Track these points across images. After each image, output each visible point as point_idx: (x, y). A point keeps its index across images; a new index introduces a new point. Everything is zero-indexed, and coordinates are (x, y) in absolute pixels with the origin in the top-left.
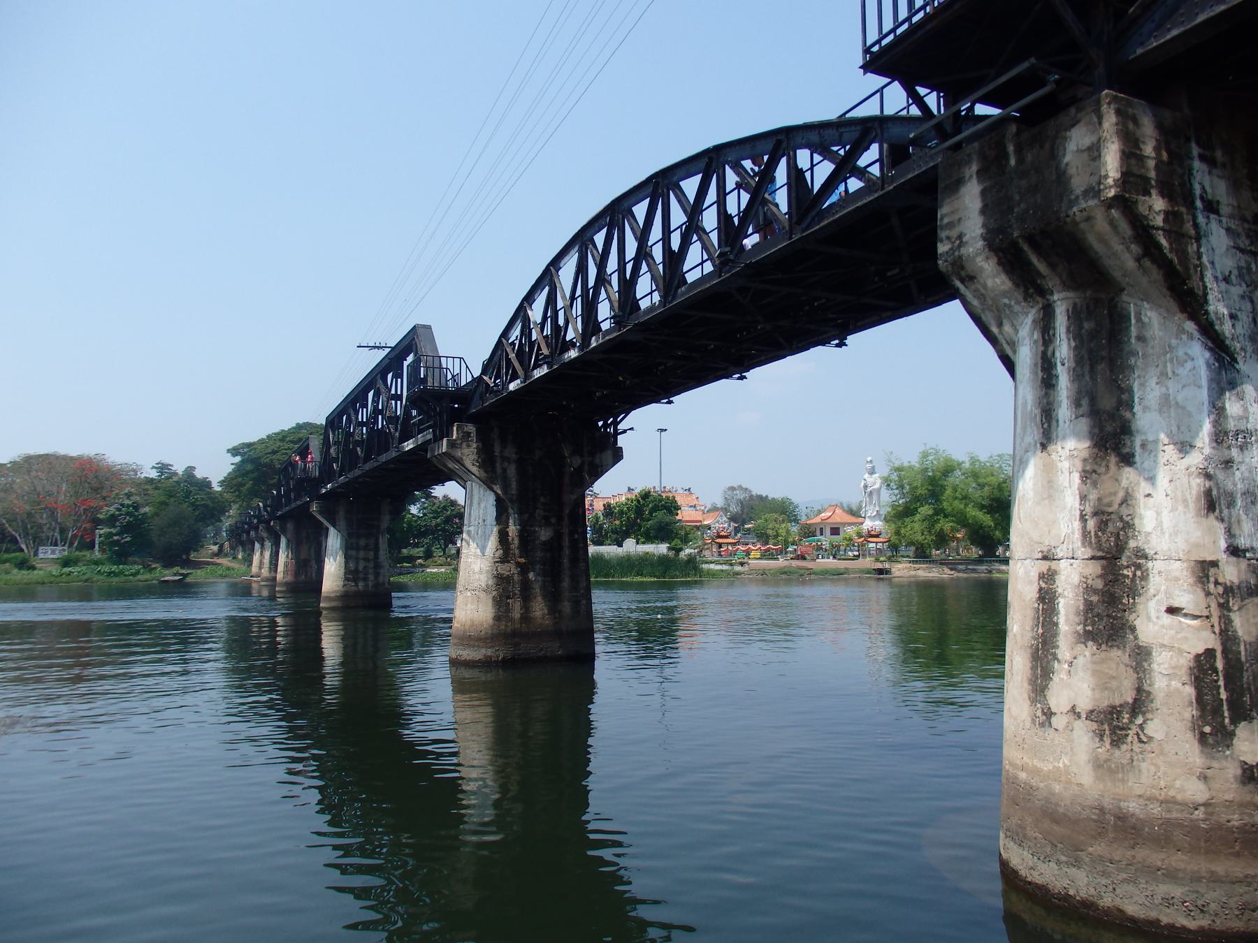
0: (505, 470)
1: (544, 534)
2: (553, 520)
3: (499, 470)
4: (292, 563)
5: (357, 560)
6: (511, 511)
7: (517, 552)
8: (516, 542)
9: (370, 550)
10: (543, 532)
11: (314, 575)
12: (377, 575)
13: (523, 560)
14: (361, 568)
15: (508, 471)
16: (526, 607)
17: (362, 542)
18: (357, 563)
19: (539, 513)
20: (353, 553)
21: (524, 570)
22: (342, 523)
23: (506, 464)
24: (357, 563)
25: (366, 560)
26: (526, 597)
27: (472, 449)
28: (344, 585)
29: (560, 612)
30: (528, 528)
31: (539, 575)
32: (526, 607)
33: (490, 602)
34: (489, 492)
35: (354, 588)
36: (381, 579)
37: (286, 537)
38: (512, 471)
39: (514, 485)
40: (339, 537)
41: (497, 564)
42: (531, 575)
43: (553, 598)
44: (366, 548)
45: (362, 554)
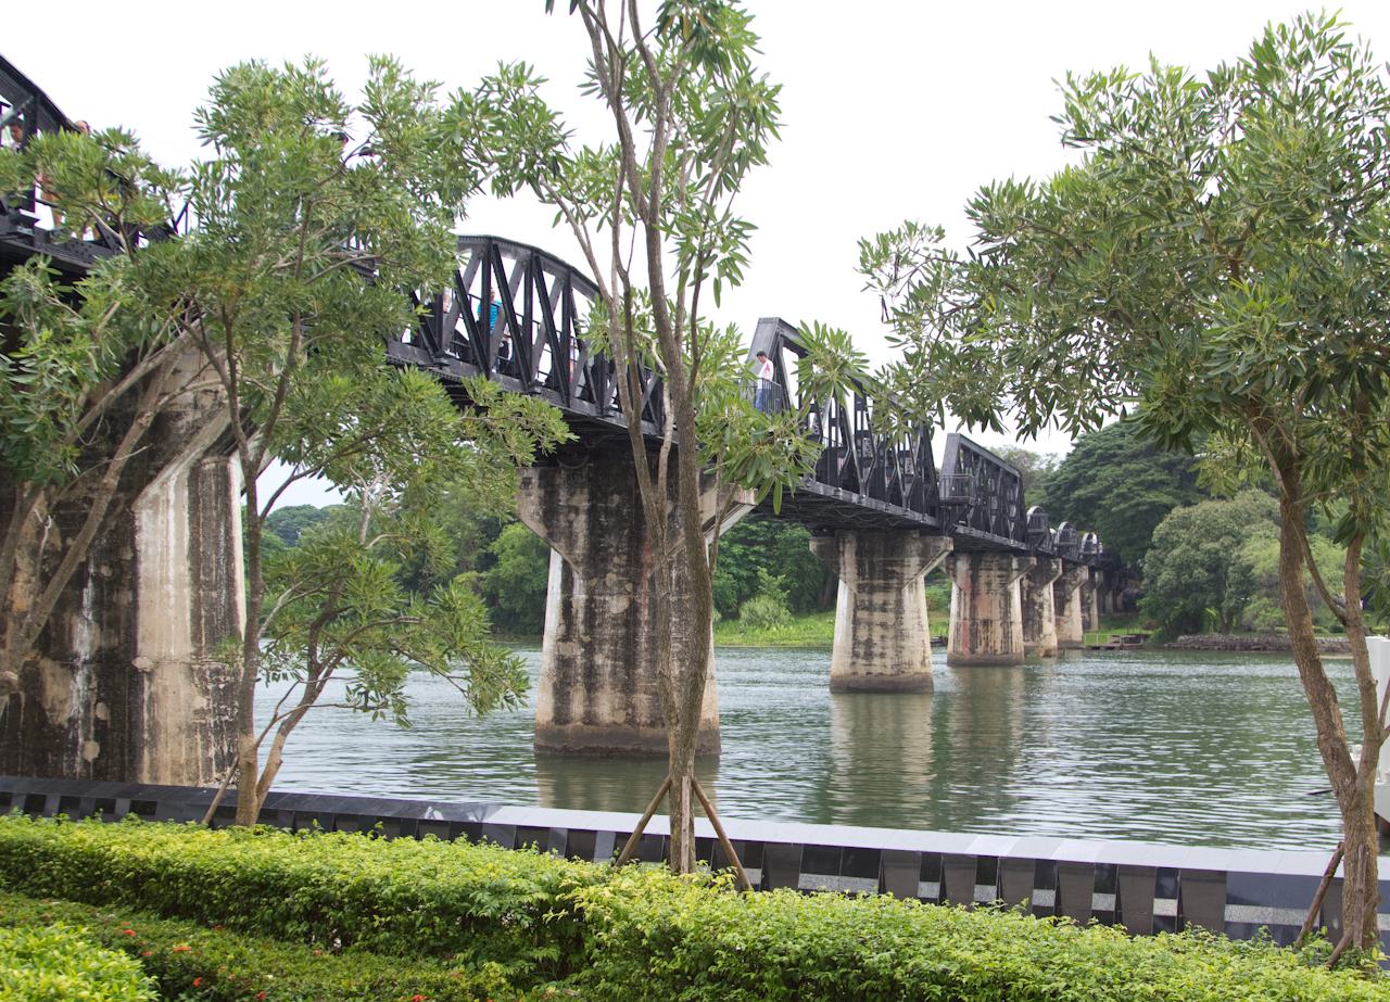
0: (571, 523)
1: (617, 605)
2: (629, 587)
3: (563, 524)
4: (965, 625)
5: (870, 624)
6: (576, 576)
7: (581, 628)
8: (581, 615)
10: (614, 602)
11: (998, 645)
12: (899, 650)
13: (587, 639)
14: (876, 639)
16: (590, 701)
17: (878, 598)
18: (870, 630)
19: (611, 578)
20: (862, 614)
21: (590, 650)
23: (572, 516)
24: (870, 630)
25: (883, 625)
26: (591, 688)
28: (854, 663)
29: (634, 707)
30: (597, 598)
31: (608, 657)
32: (590, 701)
33: (551, 689)
35: (862, 671)
36: (906, 656)
38: (581, 524)
39: (581, 542)
42: (599, 659)
43: (628, 688)
44: (884, 609)
45: (878, 617)
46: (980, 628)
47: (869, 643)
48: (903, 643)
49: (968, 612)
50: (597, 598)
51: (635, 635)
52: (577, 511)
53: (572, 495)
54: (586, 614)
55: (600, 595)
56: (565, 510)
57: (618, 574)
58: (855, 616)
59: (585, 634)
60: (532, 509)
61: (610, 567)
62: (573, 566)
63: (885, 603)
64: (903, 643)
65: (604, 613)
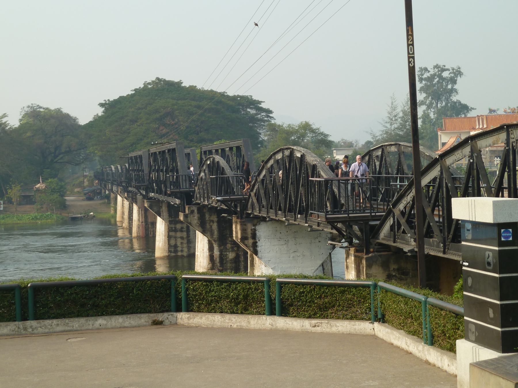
0: (211, 226)
4: (142, 225)
5: (176, 238)
7: (218, 264)
8: (218, 260)
9: (185, 231)
14: (179, 244)
15: (213, 227)
18: (176, 240)
20: (172, 234)
22: (165, 213)
23: (212, 223)
25: (182, 238)
27: (195, 217)
30: (224, 253)
34: (205, 237)
37: (136, 204)
38: (215, 226)
39: (216, 233)
40: (163, 224)
41: (209, 270)
44: (181, 230)
45: (179, 234)
46: (150, 226)
47: (176, 246)
48: (190, 245)
49: (143, 219)
50: (224, 253)
51: (239, 266)
52: (213, 221)
53: (211, 216)
54: (220, 259)
55: (225, 252)
56: (209, 222)
57: (231, 244)
58: (168, 234)
59: (220, 267)
60: (196, 222)
61: (228, 242)
62: (213, 242)
63: (182, 228)
64: (190, 245)
65: (226, 258)
